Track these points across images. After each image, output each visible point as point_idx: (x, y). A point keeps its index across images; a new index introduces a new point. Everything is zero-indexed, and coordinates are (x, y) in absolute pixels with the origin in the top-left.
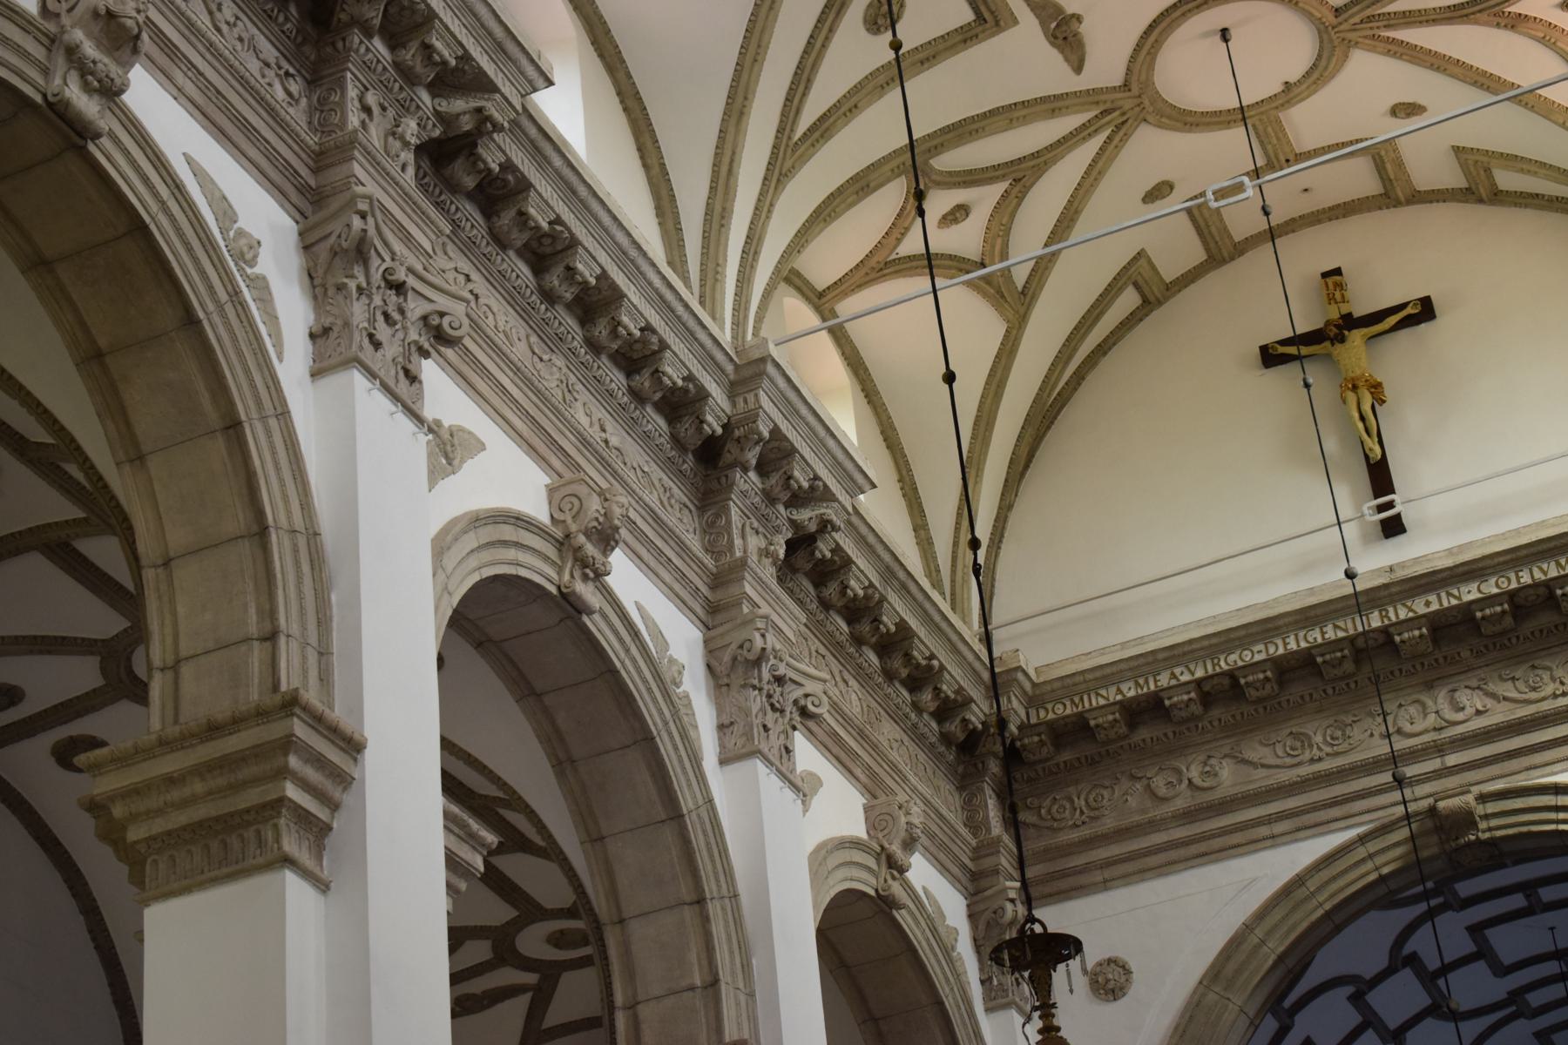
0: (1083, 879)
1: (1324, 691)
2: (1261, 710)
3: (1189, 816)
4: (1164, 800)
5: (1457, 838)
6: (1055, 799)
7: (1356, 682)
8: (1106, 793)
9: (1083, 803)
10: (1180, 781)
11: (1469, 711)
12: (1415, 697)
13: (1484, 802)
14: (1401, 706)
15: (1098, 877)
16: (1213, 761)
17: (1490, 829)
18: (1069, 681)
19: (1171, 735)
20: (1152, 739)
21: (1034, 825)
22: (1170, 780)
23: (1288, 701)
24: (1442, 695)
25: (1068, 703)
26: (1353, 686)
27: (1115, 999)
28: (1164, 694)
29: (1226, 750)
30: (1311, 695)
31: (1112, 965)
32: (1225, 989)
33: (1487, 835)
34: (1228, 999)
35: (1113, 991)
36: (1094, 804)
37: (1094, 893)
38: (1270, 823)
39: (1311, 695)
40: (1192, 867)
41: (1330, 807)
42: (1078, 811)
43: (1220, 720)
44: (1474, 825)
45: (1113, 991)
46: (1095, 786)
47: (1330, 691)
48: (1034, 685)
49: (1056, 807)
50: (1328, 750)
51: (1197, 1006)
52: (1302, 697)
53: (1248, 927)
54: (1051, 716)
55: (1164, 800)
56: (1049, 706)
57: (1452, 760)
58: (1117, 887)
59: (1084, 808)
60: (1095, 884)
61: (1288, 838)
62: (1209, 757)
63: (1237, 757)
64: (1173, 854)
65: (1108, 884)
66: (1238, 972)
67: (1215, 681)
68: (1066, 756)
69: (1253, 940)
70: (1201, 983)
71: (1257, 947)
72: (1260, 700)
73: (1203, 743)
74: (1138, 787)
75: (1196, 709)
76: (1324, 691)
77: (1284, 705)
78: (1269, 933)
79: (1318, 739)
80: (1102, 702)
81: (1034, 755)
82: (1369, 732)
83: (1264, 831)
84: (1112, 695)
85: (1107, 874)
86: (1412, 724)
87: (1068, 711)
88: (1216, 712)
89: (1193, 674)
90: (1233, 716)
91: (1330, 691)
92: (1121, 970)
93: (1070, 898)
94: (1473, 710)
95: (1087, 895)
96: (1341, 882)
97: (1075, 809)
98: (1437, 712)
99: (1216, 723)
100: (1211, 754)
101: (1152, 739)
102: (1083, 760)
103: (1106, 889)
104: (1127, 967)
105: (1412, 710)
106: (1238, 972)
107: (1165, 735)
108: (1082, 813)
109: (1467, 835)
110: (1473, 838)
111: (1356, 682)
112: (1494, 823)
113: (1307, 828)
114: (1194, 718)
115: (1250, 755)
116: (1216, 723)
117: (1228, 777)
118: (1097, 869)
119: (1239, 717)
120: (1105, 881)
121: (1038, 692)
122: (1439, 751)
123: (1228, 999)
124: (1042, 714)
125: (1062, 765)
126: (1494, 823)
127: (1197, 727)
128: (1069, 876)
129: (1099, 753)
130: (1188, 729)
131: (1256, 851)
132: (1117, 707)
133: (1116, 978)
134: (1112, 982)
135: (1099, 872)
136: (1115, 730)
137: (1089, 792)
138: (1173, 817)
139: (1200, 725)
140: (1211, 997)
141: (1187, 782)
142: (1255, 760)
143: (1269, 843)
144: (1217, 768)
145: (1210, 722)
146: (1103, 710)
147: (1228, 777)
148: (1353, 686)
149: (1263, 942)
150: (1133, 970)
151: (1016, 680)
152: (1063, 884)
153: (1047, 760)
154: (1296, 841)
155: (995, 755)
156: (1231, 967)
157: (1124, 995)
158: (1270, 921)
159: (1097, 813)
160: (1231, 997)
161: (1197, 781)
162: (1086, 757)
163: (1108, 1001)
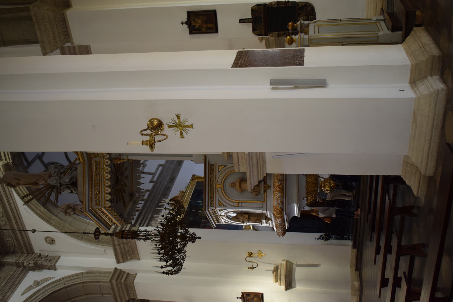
0: (26, 241)
3: (9, 219)
4: (6, 223)
5: (12, 167)
6: (7, 243)
8: (5, 234)
9: (8, 238)
13: (2, 159)
15: (25, 239)
17: (9, 159)
22: (1, 221)
27: (55, 240)
31: (47, 240)
32: (51, 219)
33: (11, 160)
35: (52, 241)
36: (8, 236)
38: (10, 203)
41: (5, 191)
44: (8, 164)
45: (52, 241)
46: (4, 235)
49: (9, 244)
51: (55, 226)
53: (36, 213)
55: (6, 223)
59: (9, 238)
60: (27, 239)
64: (19, 223)
66: (47, 216)
69: (39, 212)
70: (50, 225)
71: (41, 212)
78: (37, 209)
83: (12, 205)
85: (25, 236)
92: (47, 239)
93: (31, 244)
95: (30, 241)
97: (9, 240)
103: (29, 237)
104: (47, 237)
106: (47, 216)
108: (10, 239)
110: (11, 164)
112: (7, 158)
118: (24, 239)
120: (27, 237)
123: (54, 219)
126: (7, 158)
134: (50, 241)
137: (5, 237)
140: (53, 222)
149: (40, 210)
150: (47, 236)
152: (28, 245)
156: (47, 218)
157: (53, 239)
158: (35, 208)
159: (10, 236)
160: (53, 219)
163: (55, 242)
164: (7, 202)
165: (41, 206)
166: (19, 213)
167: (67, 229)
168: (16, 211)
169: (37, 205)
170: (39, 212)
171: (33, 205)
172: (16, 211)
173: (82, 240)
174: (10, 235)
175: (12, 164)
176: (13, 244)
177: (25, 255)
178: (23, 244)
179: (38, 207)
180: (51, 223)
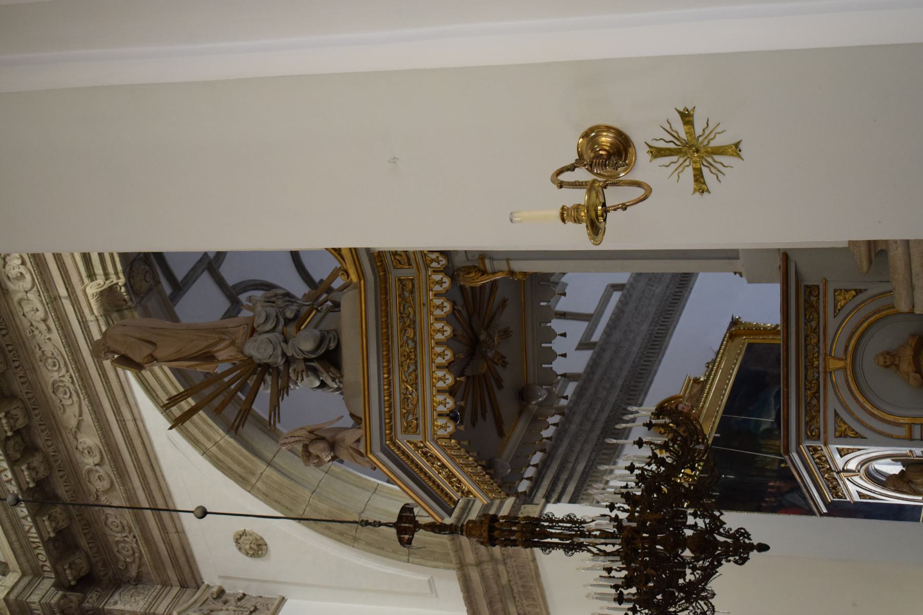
0: (177, 545)
1: (17, 368)
2: (36, 412)
4: (112, 484)
5: (125, 300)
7: (7, 345)
8: (110, 520)
9: (119, 535)
10: (97, 471)
11: (22, 269)
12: (16, 304)
13: (95, 274)
14: (24, 315)
15: (174, 537)
16: (80, 447)
17: (116, 273)
18: (19, 551)
19: (61, 473)
20: (65, 486)
21: (139, 567)
22: (97, 477)
23: (27, 393)
24: (11, 286)
25: (37, 551)
26: (10, 348)
27: (266, 545)
28: (24, 487)
29: (71, 437)
30: (21, 377)
31: (240, 541)
32: (254, 474)
33: (121, 275)
34: (262, 474)
35: (259, 545)
36: (120, 529)
37: (187, 539)
38: (124, 420)
39: (21, 377)
40: (163, 476)
41: (108, 378)
42: (125, 539)
43: (47, 440)
45: (259, 545)
46: (105, 524)
47: (17, 364)
48: (24, 574)
49: (124, 552)
50: (63, 371)
52: (23, 383)
53: (205, 452)
54: (48, 563)
55: (112, 484)
56: (41, 563)
57: (63, 292)
58: (182, 524)
59: (124, 535)
61: (135, 410)
62: (77, 448)
63: (76, 432)
64: (153, 486)
65: (179, 529)
66: (239, 464)
67: (11, 452)
68: (83, 542)
69: (214, 449)
70: (249, 492)
71: (220, 448)
72: (28, 415)
73: (67, 450)
74: (104, 498)
75: (36, 461)
76: (17, 368)
77: (30, 396)
78: (209, 438)
79: (56, 376)
80: (33, 530)
81: (83, 568)
82: (47, 341)
83: (131, 425)
84: (28, 523)
85: (171, 529)
86: (37, 310)
87: (43, 552)
88: (40, 442)
89: (6, 470)
90: (42, 431)
91: (17, 364)
92: (243, 538)
93: (192, 555)
94: (21, 266)
95: (189, 544)
96: (166, 383)
97: (124, 540)
98: (26, 292)
99: (49, 443)
100: (75, 447)
101: (65, 486)
102: (86, 531)
103: (184, 532)
104: (241, 533)
105: (27, 309)
106: (239, 464)
107: (61, 477)
109: (121, 293)
110: (123, 289)
111: (7, 345)
113: (126, 396)
114: (46, 460)
115: (73, 422)
116: (49, 443)
117: (89, 439)
118: (168, 536)
119: (43, 427)
120: (177, 532)
121: (30, 571)
122: (55, 299)
123: (262, 474)
124: (46, 569)
125: (91, 545)
127: (53, 456)
128: (175, 554)
129: (79, 521)
130: (56, 461)
131: (147, 433)
132: (38, 519)
133: (249, 543)
134: (252, 545)
135: (171, 535)
136: (58, 515)
137: (111, 529)
138: (124, 484)
139: (52, 454)
140: (259, 485)
141: (97, 467)
142: (76, 420)
143: (139, 423)
144: (85, 446)
145: (49, 446)
146: (41, 528)
147: (89, 439)
148: (10, 348)
149: (216, 443)
150: (243, 529)
151: (16, 599)
153: (87, 556)
154: (136, 404)
155: (82, 602)
157: (262, 539)
159: (126, 528)
160: (260, 472)
161: (97, 459)
162: (83, 529)
163: (267, 550)
164: (114, 417)
165: (221, 431)
166: (150, 452)
167: (306, 506)
168: (143, 443)
169: (208, 425)
170: (214, 449)
171: (197, 427)
172: (143, 443)
173: (355, 545)
174: (125, 523)
175: (127, 291)
176: (137, 555)
177: (176, 590)
178: (166, 553)
179: (211, 433)
180: (253, 487)
